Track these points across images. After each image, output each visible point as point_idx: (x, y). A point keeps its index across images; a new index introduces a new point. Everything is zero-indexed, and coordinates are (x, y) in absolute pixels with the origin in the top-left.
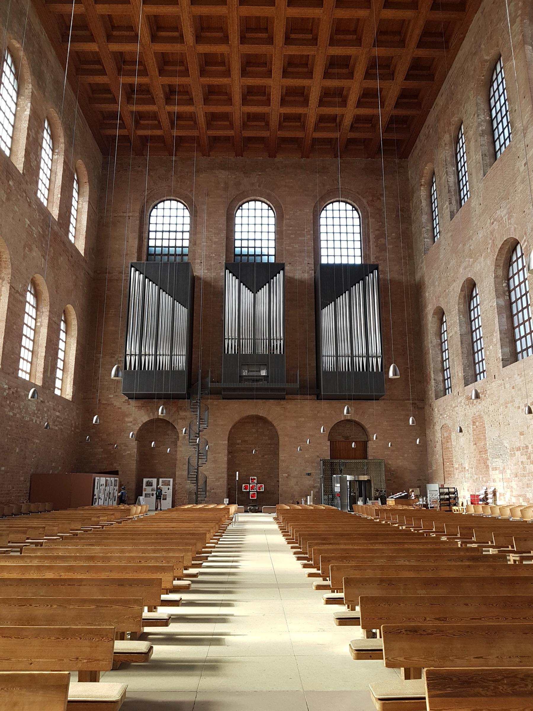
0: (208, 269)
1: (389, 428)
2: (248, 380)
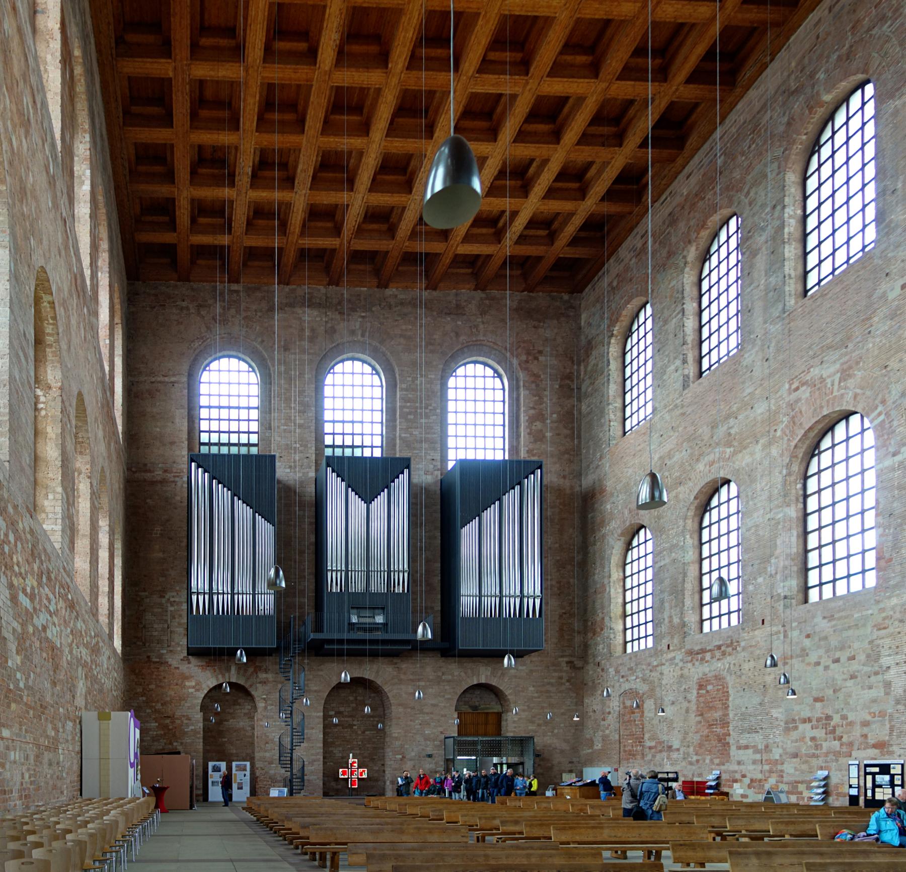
0: (290, 467)
1: (536, 695)
2: (359, 629)
